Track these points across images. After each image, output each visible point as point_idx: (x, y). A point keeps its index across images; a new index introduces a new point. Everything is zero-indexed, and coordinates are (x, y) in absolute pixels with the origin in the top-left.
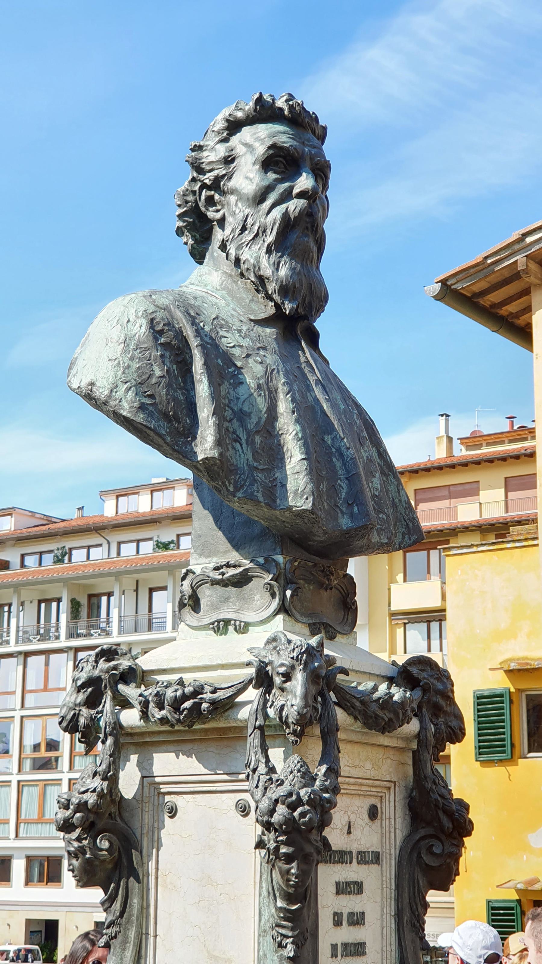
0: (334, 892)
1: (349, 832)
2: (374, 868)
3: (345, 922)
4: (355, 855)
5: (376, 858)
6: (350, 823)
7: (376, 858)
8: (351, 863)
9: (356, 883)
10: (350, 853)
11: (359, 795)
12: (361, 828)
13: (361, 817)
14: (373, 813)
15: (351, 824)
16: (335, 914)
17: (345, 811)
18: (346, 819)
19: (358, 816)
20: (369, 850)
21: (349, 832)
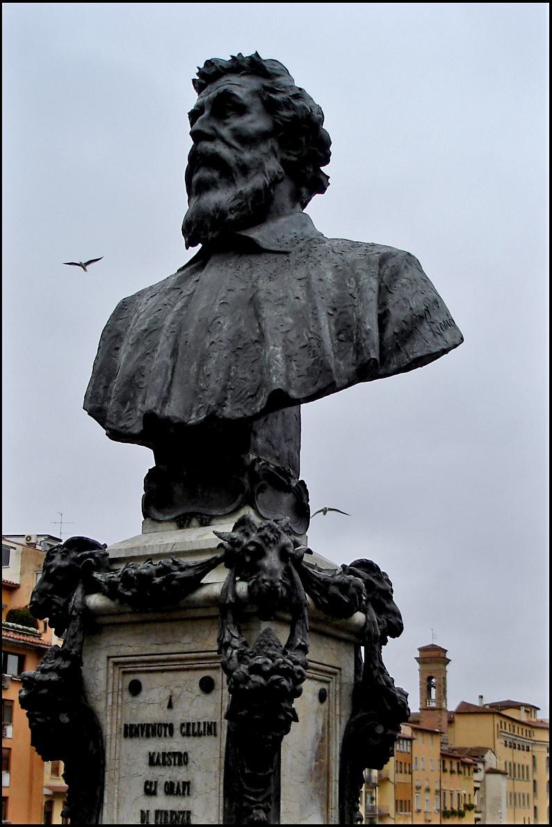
0: (148, 762)
1: (170, 706)
2: (207, 741)
3: (160, 791)
4: (177, 727)
5: (210, 729)
6: (171, 696)
7: (210, 729)
8: (171, 734)
9: (179, 754)
10: (171, 727)
11: (187, 670)
12: (190, 700)
13: (190, 690)
14: (207, 686)
15: (173, 698)
16: (147, 783)
17: (166, 687)
18: (168, 694)
19: (185, 689)
20: (201, 721)
21: (170, 706)
